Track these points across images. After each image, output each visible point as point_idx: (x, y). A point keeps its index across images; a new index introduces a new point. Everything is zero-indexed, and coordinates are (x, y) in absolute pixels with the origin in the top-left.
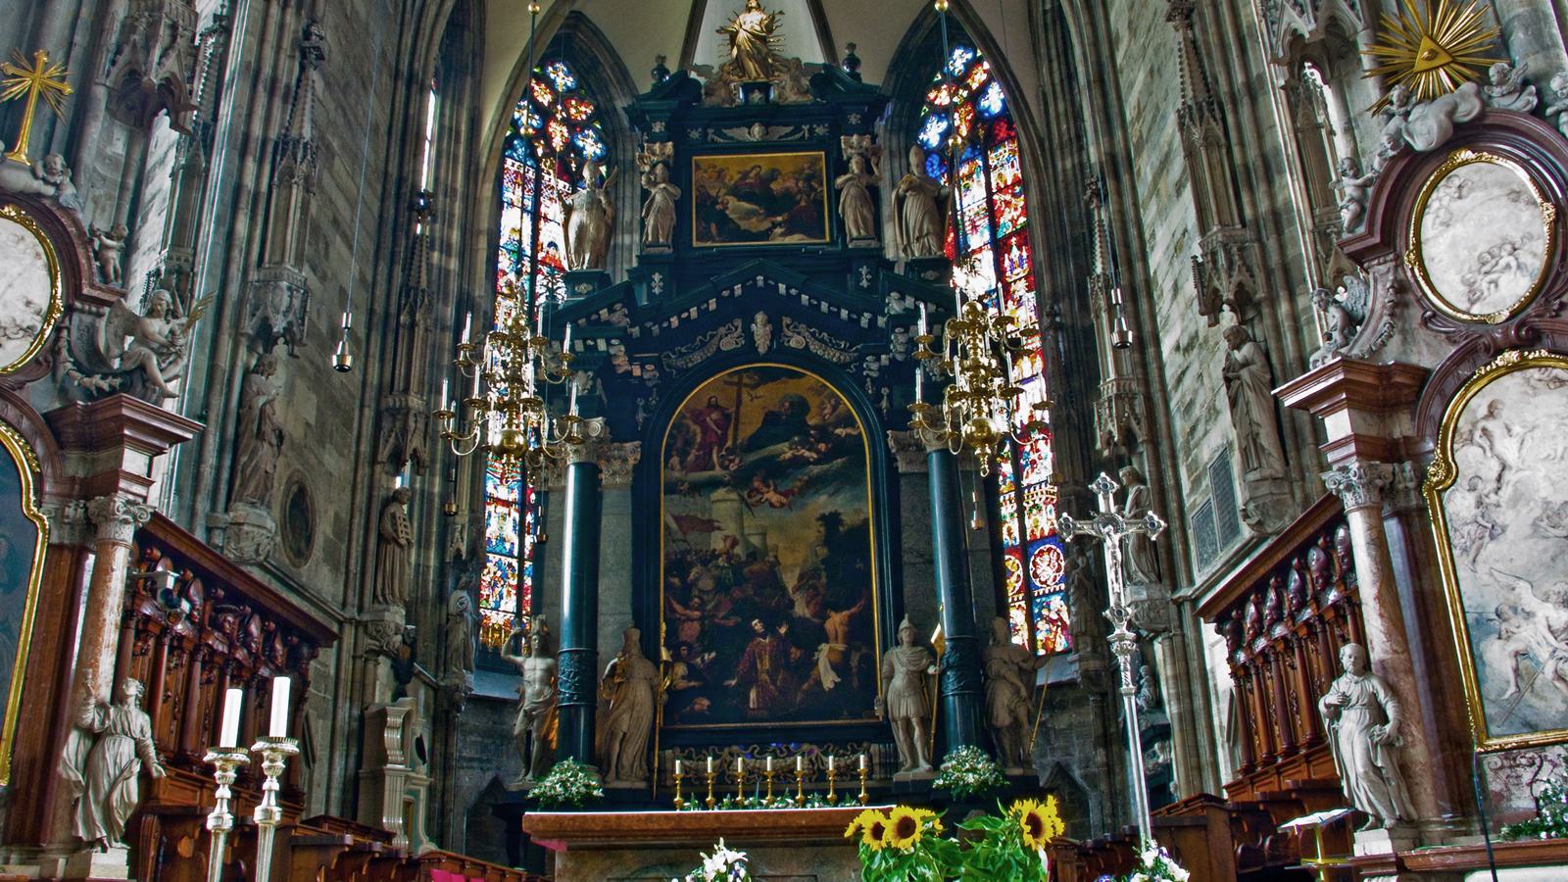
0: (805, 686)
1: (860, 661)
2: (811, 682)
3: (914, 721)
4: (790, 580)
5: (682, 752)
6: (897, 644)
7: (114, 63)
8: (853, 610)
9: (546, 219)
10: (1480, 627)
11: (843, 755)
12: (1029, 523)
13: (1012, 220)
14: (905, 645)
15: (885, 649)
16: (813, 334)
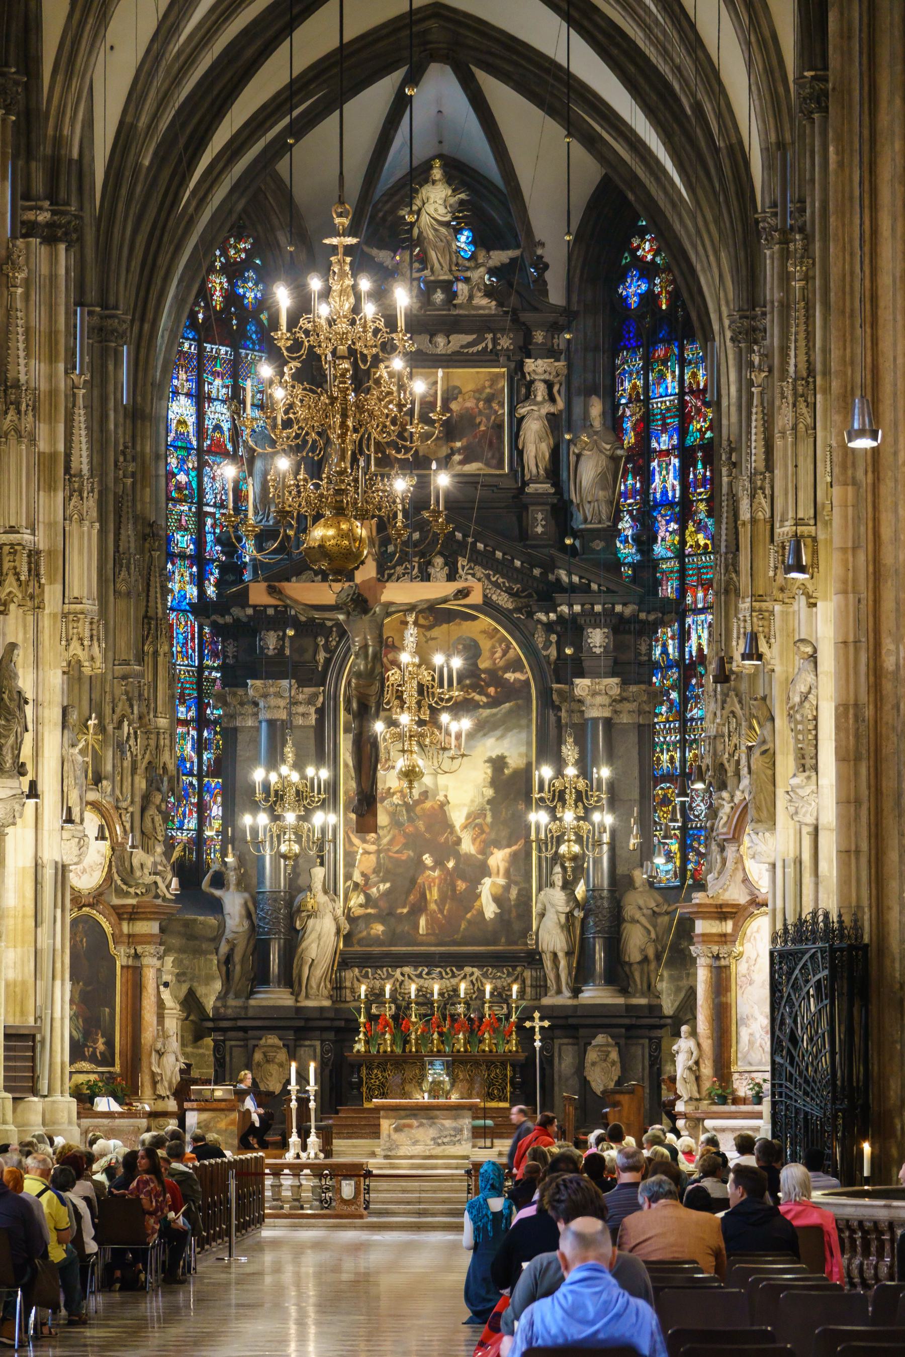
0: (469, 916)
1: (519, 894)
2: (474, 912)
3: (561, 955)
4: (458, 817)
5: (361, 972)
6: (552, 885)
7: (114, 712)
8: (514, 848)
9: (211, 400)
10: (744, 1021)
11: (500, 978)
12: (689, 755)
13: (700, 430)
14: (558, 889)
15: (540, 889)
16: (488, 577)
